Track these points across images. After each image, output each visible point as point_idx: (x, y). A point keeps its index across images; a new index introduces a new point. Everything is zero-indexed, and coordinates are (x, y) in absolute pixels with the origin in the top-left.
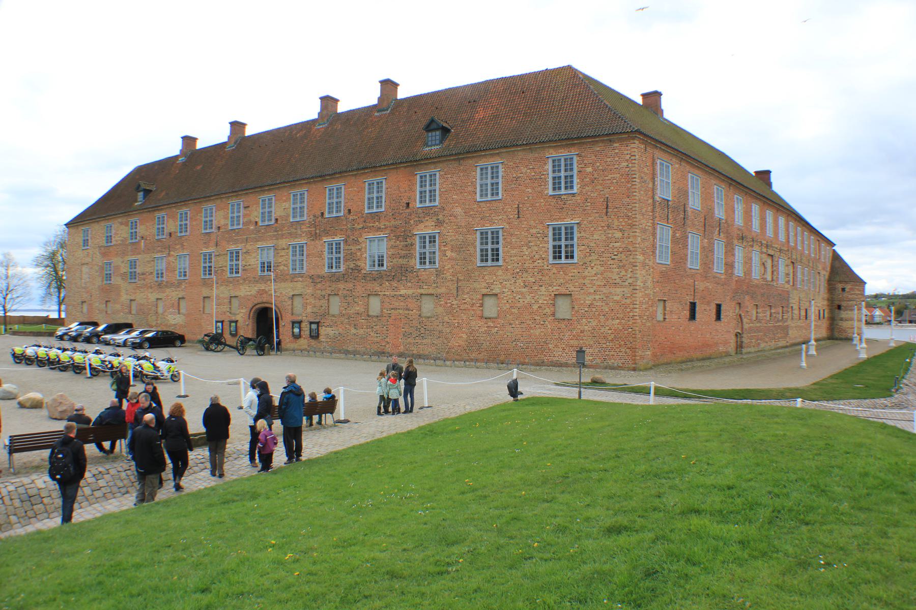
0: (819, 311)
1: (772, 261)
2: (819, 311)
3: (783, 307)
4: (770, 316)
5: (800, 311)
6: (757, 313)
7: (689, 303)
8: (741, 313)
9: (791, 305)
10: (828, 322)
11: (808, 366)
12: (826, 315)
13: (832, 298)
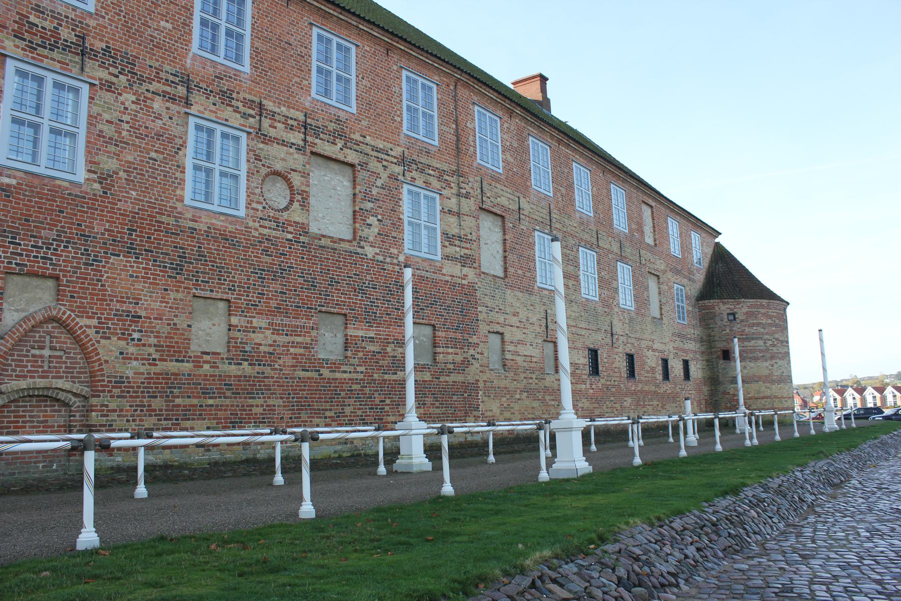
0: (665, 362)
2: (665, 362)
6: (230, 327)
8: (64, 311)
12: (696, 370)
13: (710, 336)
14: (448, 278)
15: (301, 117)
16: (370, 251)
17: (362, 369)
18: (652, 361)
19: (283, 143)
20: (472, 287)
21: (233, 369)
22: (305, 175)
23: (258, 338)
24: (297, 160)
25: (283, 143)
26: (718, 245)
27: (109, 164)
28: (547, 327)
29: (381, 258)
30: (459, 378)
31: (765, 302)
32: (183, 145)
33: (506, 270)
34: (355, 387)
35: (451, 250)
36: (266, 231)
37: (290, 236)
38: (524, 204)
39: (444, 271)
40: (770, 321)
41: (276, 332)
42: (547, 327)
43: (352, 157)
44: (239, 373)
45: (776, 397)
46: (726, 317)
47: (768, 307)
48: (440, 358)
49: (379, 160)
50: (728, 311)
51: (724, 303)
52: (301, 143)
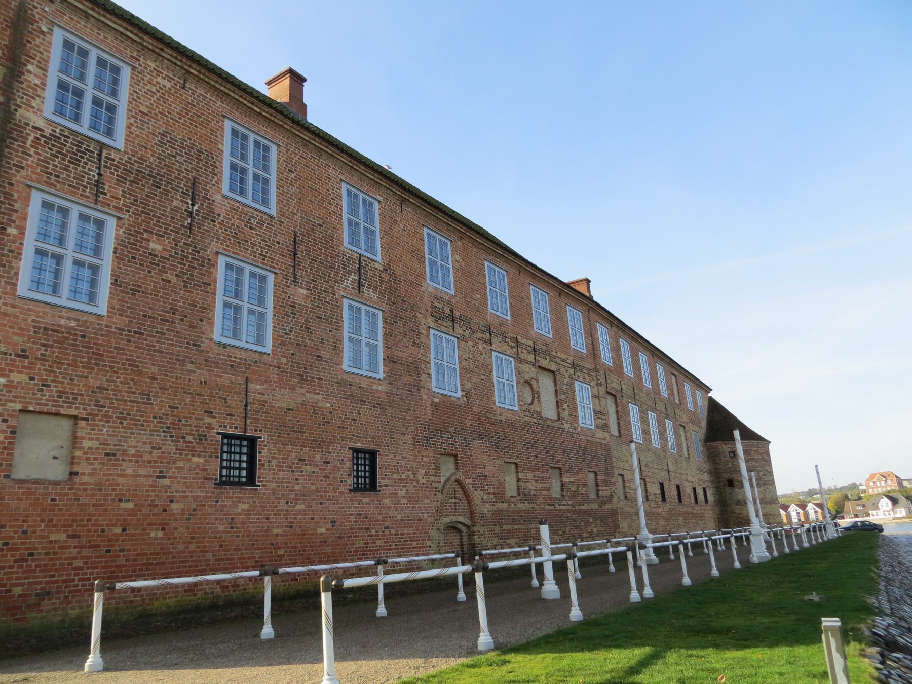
0: (694, 489)
1: (555, 382)
2: (694, 489)
3: (595, 473)
4: (562, 490)
5: (645, 485)
6: (518, 480)
7: (219, 438)
8: (460, 476)
9: (616, 472)
10: (717, 509)
11: (277, 635)
12: (711, 498)
16: (566, 426)
17: (570, 503)
18: (687, 490)
21: (521, 506)
22: (537, 381)
26: (711, 399)
27: (468, 386)
29: (571, 430)
31: (755, 442)
33: (620, 431)
36: (526, 418)
37: (535, 421)
39: (597, 436)
40: (760, 457)
41: (536, 481)
43: (553, 367)
44: (524, 508)
45: (770, 515)
46: (727, 454)
47: (758, 446)
48: (601, 493)
50: (729, 450)
51: (726, 444)
52: (533, 361)
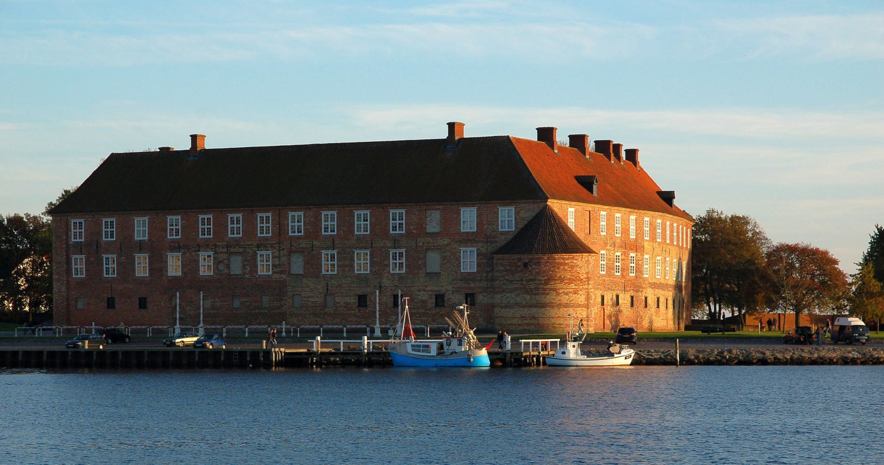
14: (275, 279)
15: (226, 243)
19: (221, 253)
20: (284, 281)
23: (217, 304)
24: (225, 256)
25: (221, 253)
27: (185, 270)
28: (327, 289)
30: (279, 311)
32: (199, 262)
34: (242, 315)
35: (276, 270)
36: (218, 277)
38: (315, 243)
39: (273, 277)
42: (327, 289)
43: (241, 250)
45: (503, 317)
49: (249, 248)
